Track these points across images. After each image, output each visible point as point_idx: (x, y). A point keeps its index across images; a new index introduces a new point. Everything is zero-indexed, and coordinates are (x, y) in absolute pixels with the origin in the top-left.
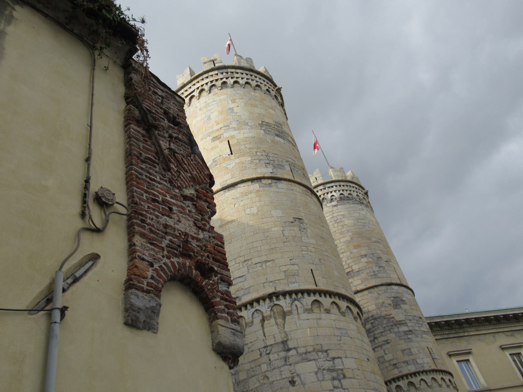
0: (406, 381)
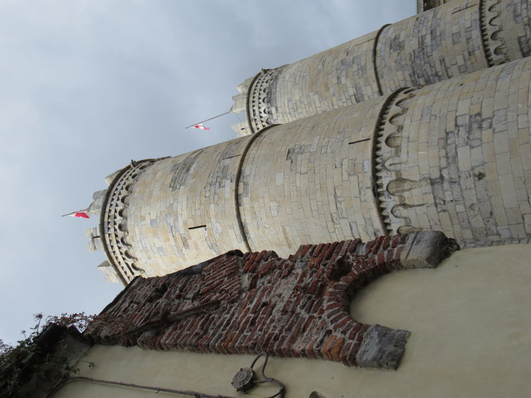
0: (490, 42)
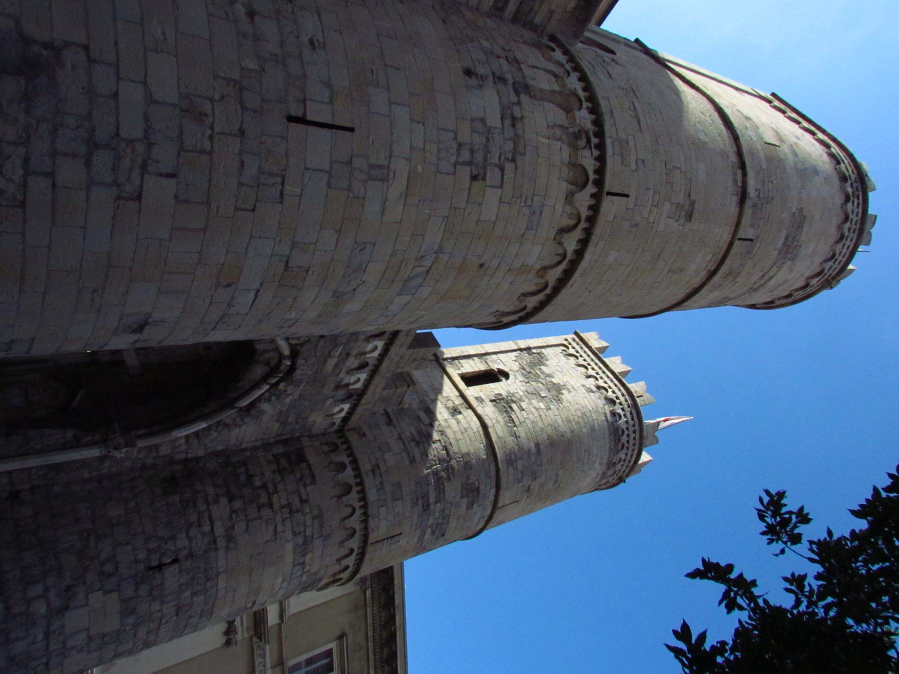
0: (352, 481)
